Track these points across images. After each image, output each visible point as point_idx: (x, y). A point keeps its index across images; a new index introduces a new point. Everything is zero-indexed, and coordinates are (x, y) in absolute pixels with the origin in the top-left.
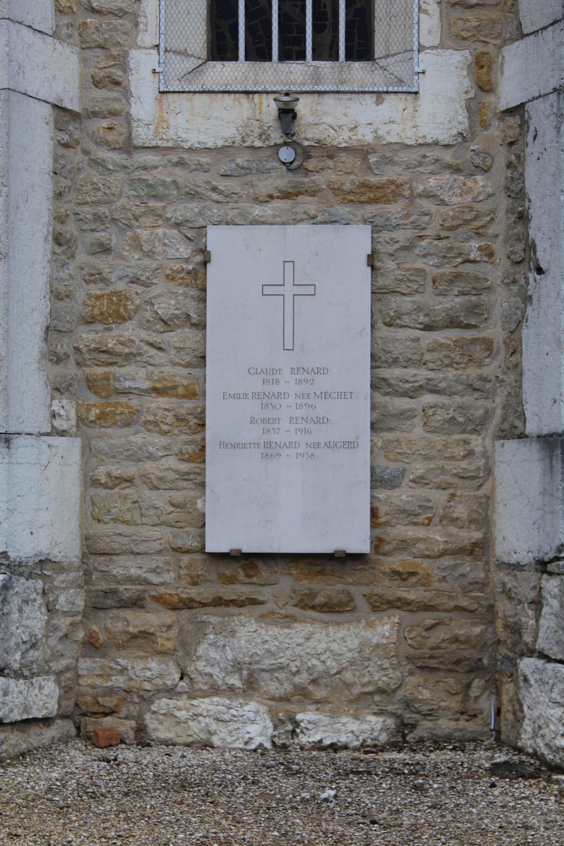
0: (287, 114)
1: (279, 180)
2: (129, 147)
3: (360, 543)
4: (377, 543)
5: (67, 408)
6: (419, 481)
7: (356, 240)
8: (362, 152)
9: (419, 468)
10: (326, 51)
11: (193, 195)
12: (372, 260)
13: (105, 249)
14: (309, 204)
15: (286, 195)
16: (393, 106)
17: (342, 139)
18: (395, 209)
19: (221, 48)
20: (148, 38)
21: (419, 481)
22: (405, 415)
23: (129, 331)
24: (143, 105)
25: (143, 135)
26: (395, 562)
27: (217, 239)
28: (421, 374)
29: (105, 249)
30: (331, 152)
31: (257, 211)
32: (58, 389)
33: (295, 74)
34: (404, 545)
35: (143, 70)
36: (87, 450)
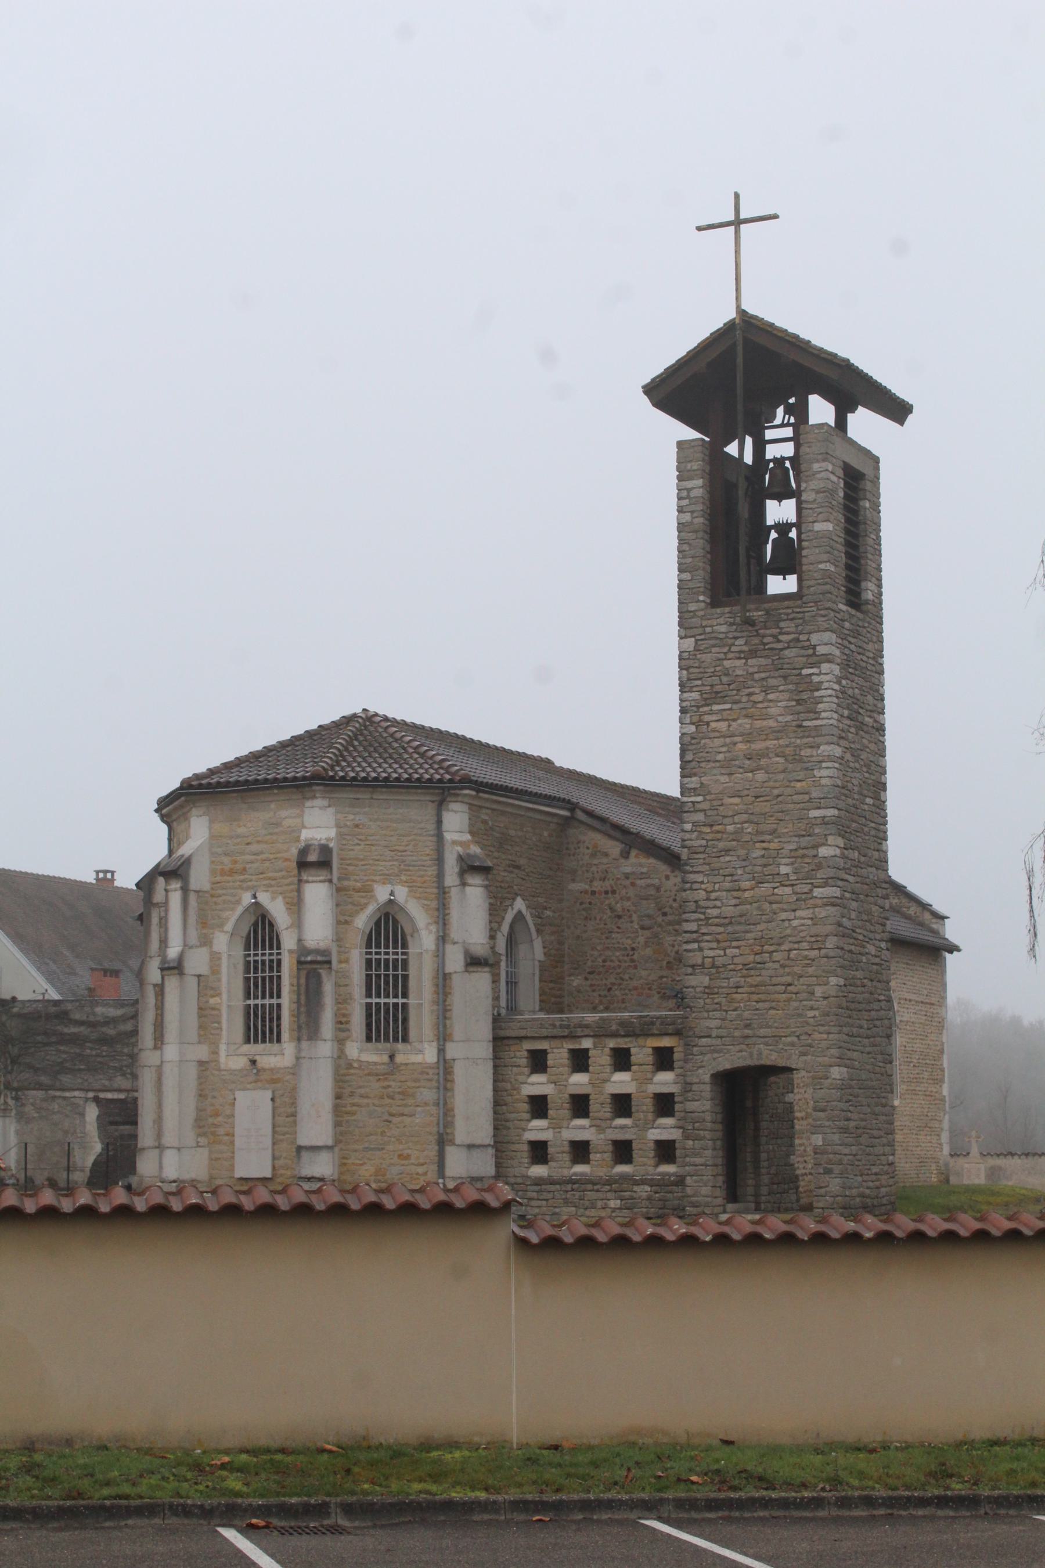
0: (254, 1062)
1: (251, 1078)
2: (219, 1070)
3: (269, 1176)
4: (274, 1175)
5: (203, 1140)
6: (285, 1158)
7: (269, 1094)
8: (271, 1070)
9: (284, 1155)
10: (271, 1041)
11: (234, 1082)
12: (273, 1100)
13: (214, 1097)
14: (259, 1084)
15: (255, 1082)
16: (279, 1058)
17: (267, 1066)
18: (279, 1085)
19: (248, 1041)
20: (224, 1041)
21: (285, 1158)
22: (281, 1140)
23: (220, 1119)
24: (222, 1058)
25: (223, 1067)
26: (279, 1180)
27: (239, 1095)
28: (286, 1129)
29: (214, 1097)
30: (264, 1070)
31: (248, 1086)
32: (199, 1135)
33: (260, 1047)
34: (281, 1175)
35: (223, 1048)
36: (210, 1152)
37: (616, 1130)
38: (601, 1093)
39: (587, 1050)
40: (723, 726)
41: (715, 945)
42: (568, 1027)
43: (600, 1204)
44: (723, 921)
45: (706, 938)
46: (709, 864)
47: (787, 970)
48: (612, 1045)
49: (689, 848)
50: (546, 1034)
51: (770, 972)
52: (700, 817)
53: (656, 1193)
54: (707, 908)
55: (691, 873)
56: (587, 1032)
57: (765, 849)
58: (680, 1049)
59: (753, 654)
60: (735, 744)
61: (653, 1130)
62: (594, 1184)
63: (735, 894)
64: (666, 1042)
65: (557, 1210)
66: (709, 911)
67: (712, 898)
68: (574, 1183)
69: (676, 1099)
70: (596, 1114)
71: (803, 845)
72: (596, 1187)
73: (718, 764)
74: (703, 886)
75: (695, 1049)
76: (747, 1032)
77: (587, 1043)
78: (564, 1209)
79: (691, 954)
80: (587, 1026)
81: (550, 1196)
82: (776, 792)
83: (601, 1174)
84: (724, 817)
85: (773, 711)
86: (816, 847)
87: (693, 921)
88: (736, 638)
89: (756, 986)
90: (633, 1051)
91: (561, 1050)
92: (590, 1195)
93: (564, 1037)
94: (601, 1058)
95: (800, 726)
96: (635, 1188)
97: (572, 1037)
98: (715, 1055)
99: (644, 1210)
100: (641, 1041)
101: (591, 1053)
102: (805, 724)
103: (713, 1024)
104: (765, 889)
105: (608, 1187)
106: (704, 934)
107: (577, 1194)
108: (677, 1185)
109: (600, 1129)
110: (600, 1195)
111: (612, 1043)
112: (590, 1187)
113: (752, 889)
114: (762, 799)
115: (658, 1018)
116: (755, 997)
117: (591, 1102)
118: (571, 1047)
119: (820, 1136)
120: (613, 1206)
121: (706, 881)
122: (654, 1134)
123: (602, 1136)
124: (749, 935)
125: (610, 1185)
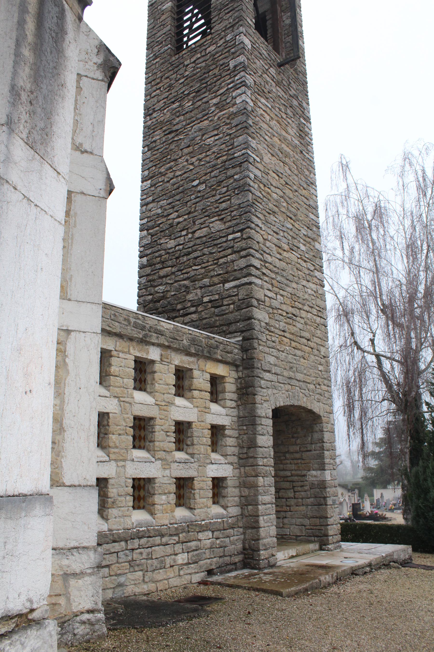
37: (181, 465)
38: (166, 418)
39: (153, 362)
40: (268, 118)
41: (270, 287)
42: (143, 328)
43: (168, 561)
44: (275, 269)
45: (266, 278)
46: (265, 216)
47: (308, 327)
48: (177, 362)
49: (253, 194)
50: (118, 330)
51: (299, 326)
52: (259, 173)
53: (217, 539)
54: (265, 252)
55: (254, 215)
56: (162, 340)
57: (293, 225)
58: (232, 380)
59: (278, 84)
60: (274, 136)
61: (211, 466)
62: (162, 536)
63: (280, 250)
64: (220, 370)
65: (122, 579)
66: (267, 256)
67: (267, 245)
68: (140, 538)
69: (227, 432)
70: (162, 444)
71: (309, 235)
72: (164, 540)
73: (266, 143)
74: (262, 233)
75: (263, 382)
76: (292, 374)
77: (154, 354)
78: (129, 575)
79: (256, 288)
80: (160, 333)
81: (113, 558)
82: (295, 187)
83: (166, 522)
84: (272, 185)
85: (290, 130)
86: (314, 240)
87: (257, 258)
88: (271, 66)
89: (293, 334)
90: (196, 373)
91: (128, 356)
92: (159, 551)
93: (131, 339)
94: (164, 376)
95: (301, 152)
96: (201, 536)
97: (144, 342)
98: (275, 391)
99: (208, 561)
100: (201, 362)
101: (157, 367)
102: (304, 152)
103: (272, 360)
104: (293, 256)
105: (176, 538)
106: (264, 274)
107: (145, 552)
108: (233, 528)
109: (166, 464)
110: (169, 550)
111: (178, 360)
112: (157, 540)
113: (287, 252)
114: (288, 186)
115: (221, 343)
116: (294, 344)
117: (157, 428)
118: (138, 354)
119: (329, 471)
120: (180, 562)
121: (263, 229)
122: (213, 471)
123: (167, 472)
124: (288, 289)
125: (177, 535)
